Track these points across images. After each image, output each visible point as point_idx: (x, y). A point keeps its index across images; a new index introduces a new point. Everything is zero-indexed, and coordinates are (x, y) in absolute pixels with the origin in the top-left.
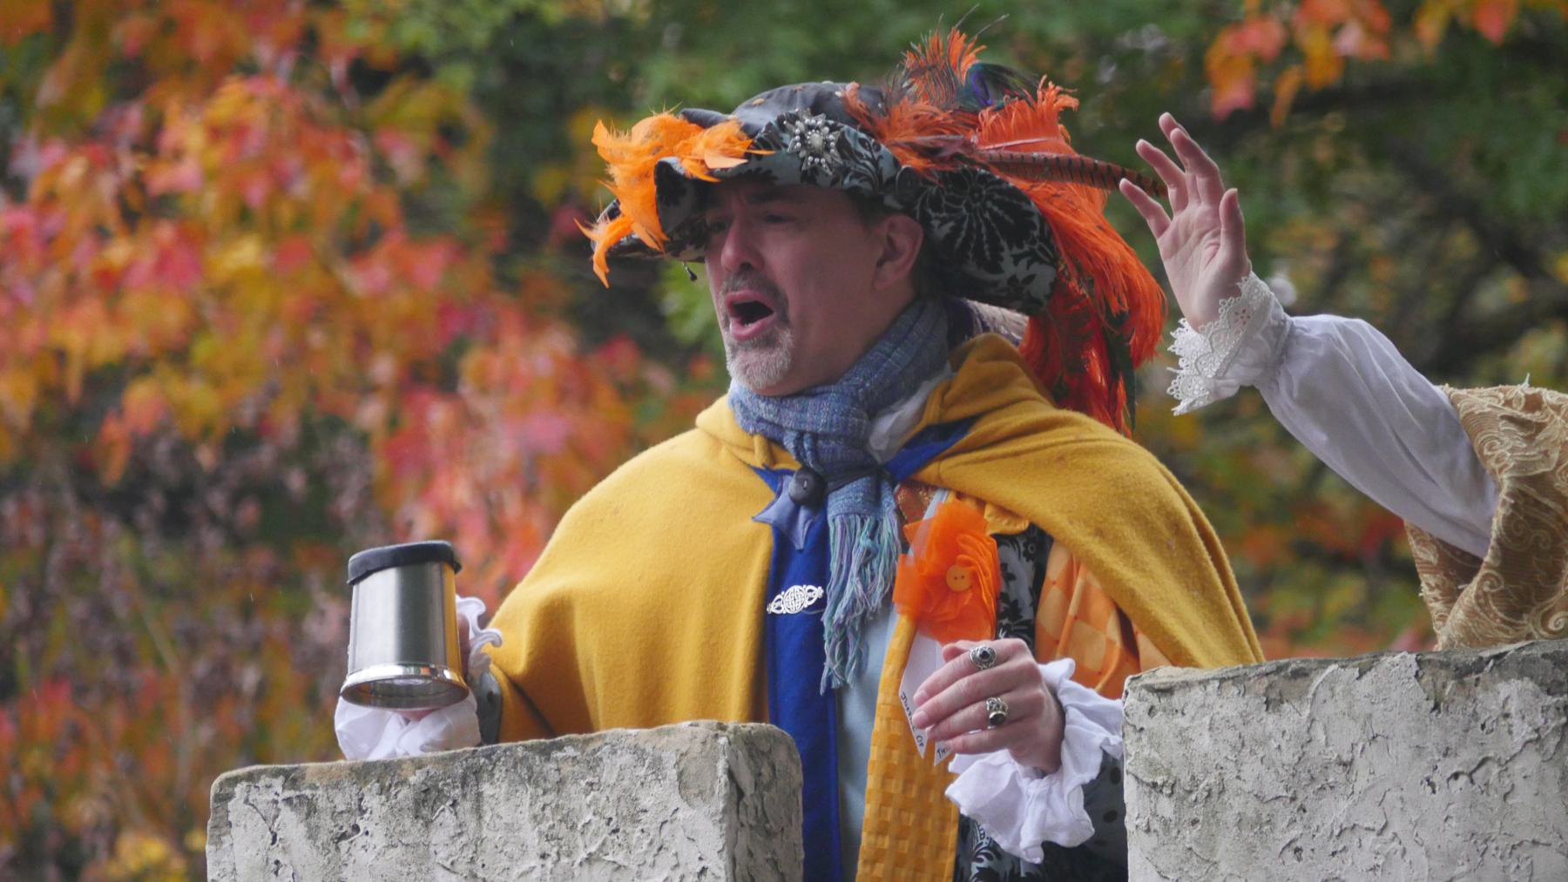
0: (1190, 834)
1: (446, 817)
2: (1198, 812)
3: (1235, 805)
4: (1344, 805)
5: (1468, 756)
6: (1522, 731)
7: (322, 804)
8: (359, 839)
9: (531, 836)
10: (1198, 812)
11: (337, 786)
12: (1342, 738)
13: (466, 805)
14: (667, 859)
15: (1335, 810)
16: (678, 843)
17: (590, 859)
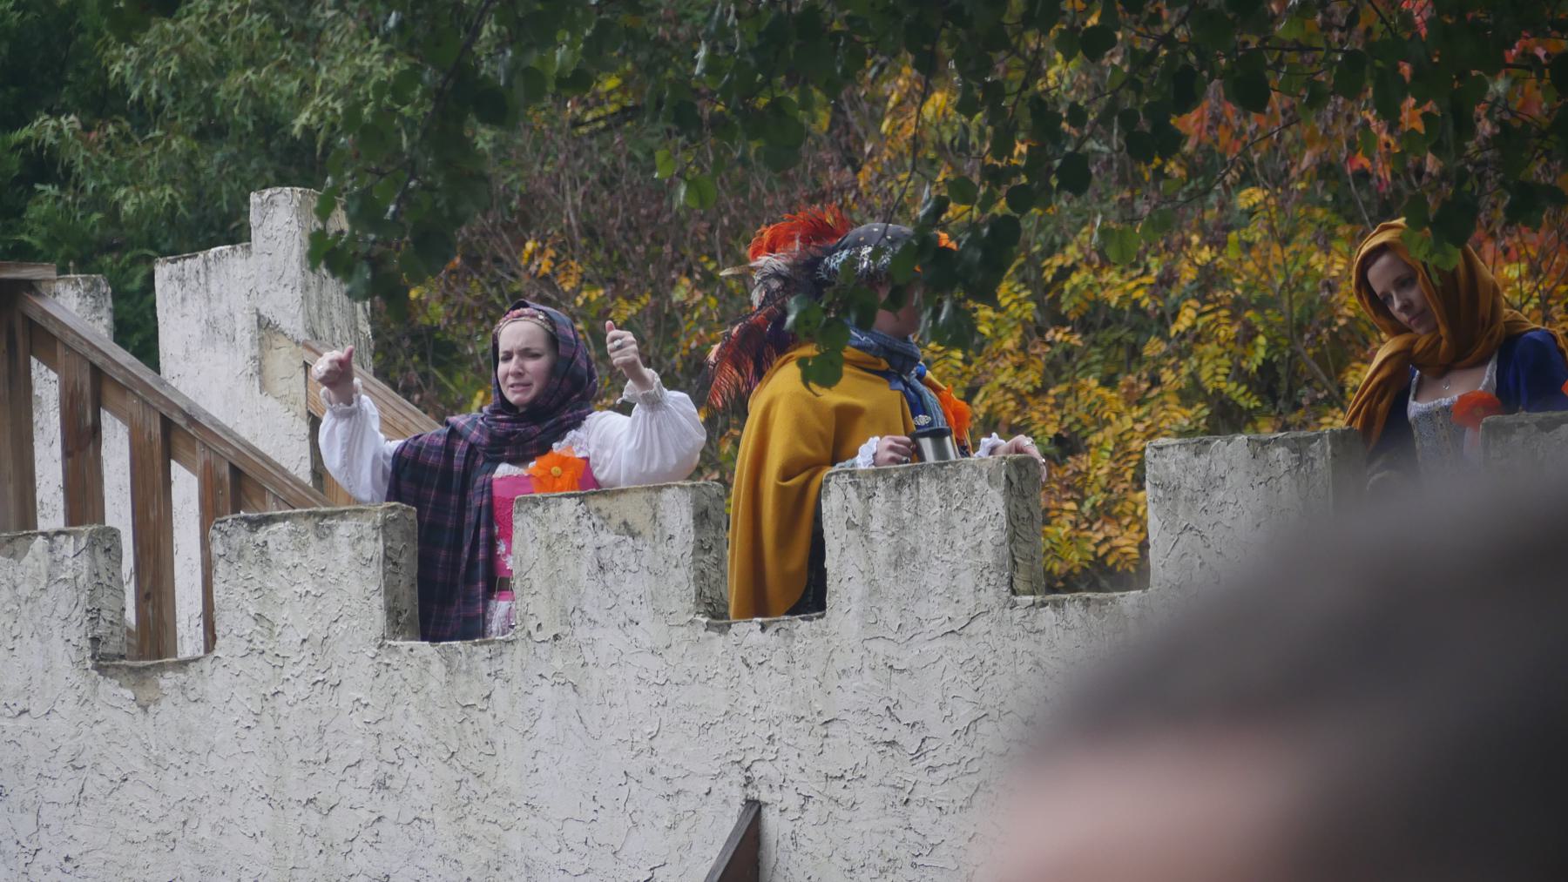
0: (1168, 504)
1: (906, 490)
2: (1171, 495)
3: (1184, 493)
5: (1265, 476)
6: (1284, 467)
9: (936, 498)
10: (1171, 495)
11: (868, 477)
12: (1222, 468)
13: (914, 486)
14: (984, 509)
15: (1219, 496)
16: (988, 503)
17: (958, 508)
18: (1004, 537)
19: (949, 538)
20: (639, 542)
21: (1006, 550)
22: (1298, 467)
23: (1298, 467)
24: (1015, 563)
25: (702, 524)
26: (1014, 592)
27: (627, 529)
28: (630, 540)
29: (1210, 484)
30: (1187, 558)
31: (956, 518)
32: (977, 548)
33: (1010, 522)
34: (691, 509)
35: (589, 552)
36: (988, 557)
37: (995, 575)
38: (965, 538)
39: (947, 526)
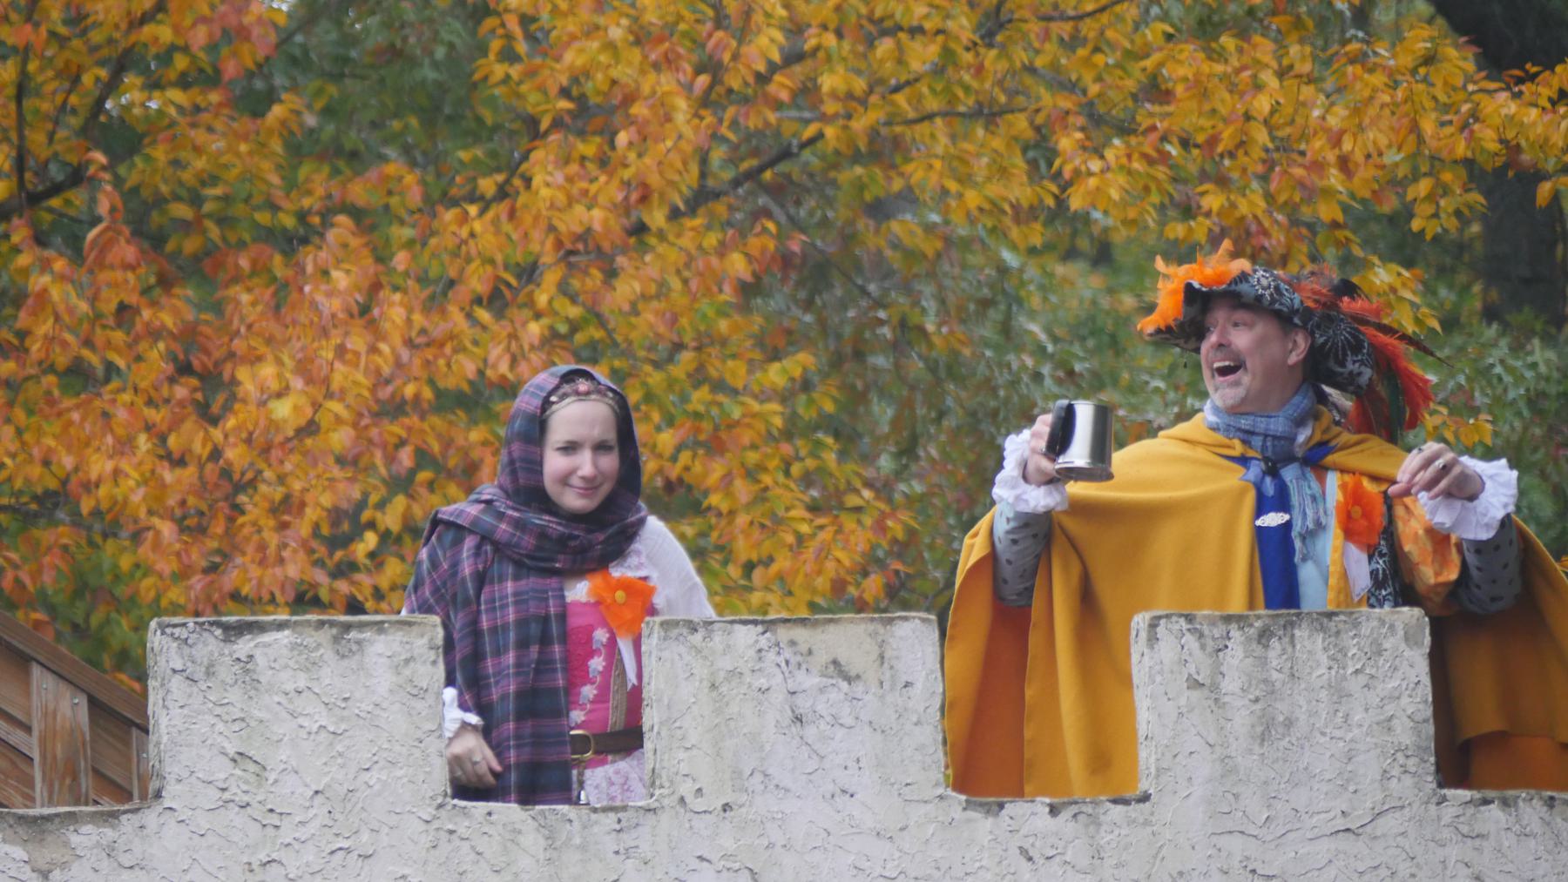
1: (1274, 642)
9: (1324, 659)
13: (1286, 640)
14: (1399, 674)
17: (1357, 672)
20: (859, 688)
31: (1355, 684)
32: (1387, 724)
35: (778, 697)
36: (1404, 734)
38: (1367, 710)
39: (1339, 693)
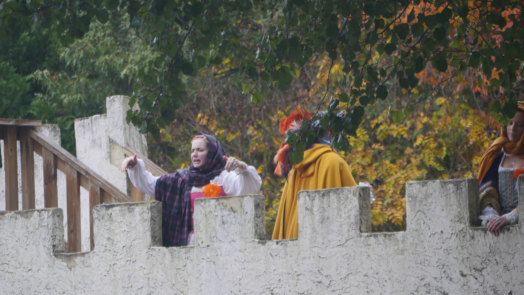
0: (413, 203)
1: (325, 198)
3: (418, 199)
4: (431, 199)
5: (446, 194)
6: (452, 191)
7: (311, 195)
8: (315, 200)
9: (336, 200)
12: (431, 191)
13: (328, 196)
14: (351, 204)
15: (430, 200)
16: (353, 202)
17: (343, 204)
18: (358, 213)
19: (340, 214)
20: (236, 214)
21: (358, 218)
22: (457, 191)
23: (457, 191)
24: (361, 222)
25: (257, 208)
26: (361, 232)
27: (232, 210)
28: (233, 213)
29: (427, 196)
30: (419, 221)
31: (342, 207)
32: (349, 217)
33: (360, 208)
34: (254, 204)
35: (219, 217)
36: (353, 220)
37: (355, 226)
38: (345, 214)
39: (339, 210)
